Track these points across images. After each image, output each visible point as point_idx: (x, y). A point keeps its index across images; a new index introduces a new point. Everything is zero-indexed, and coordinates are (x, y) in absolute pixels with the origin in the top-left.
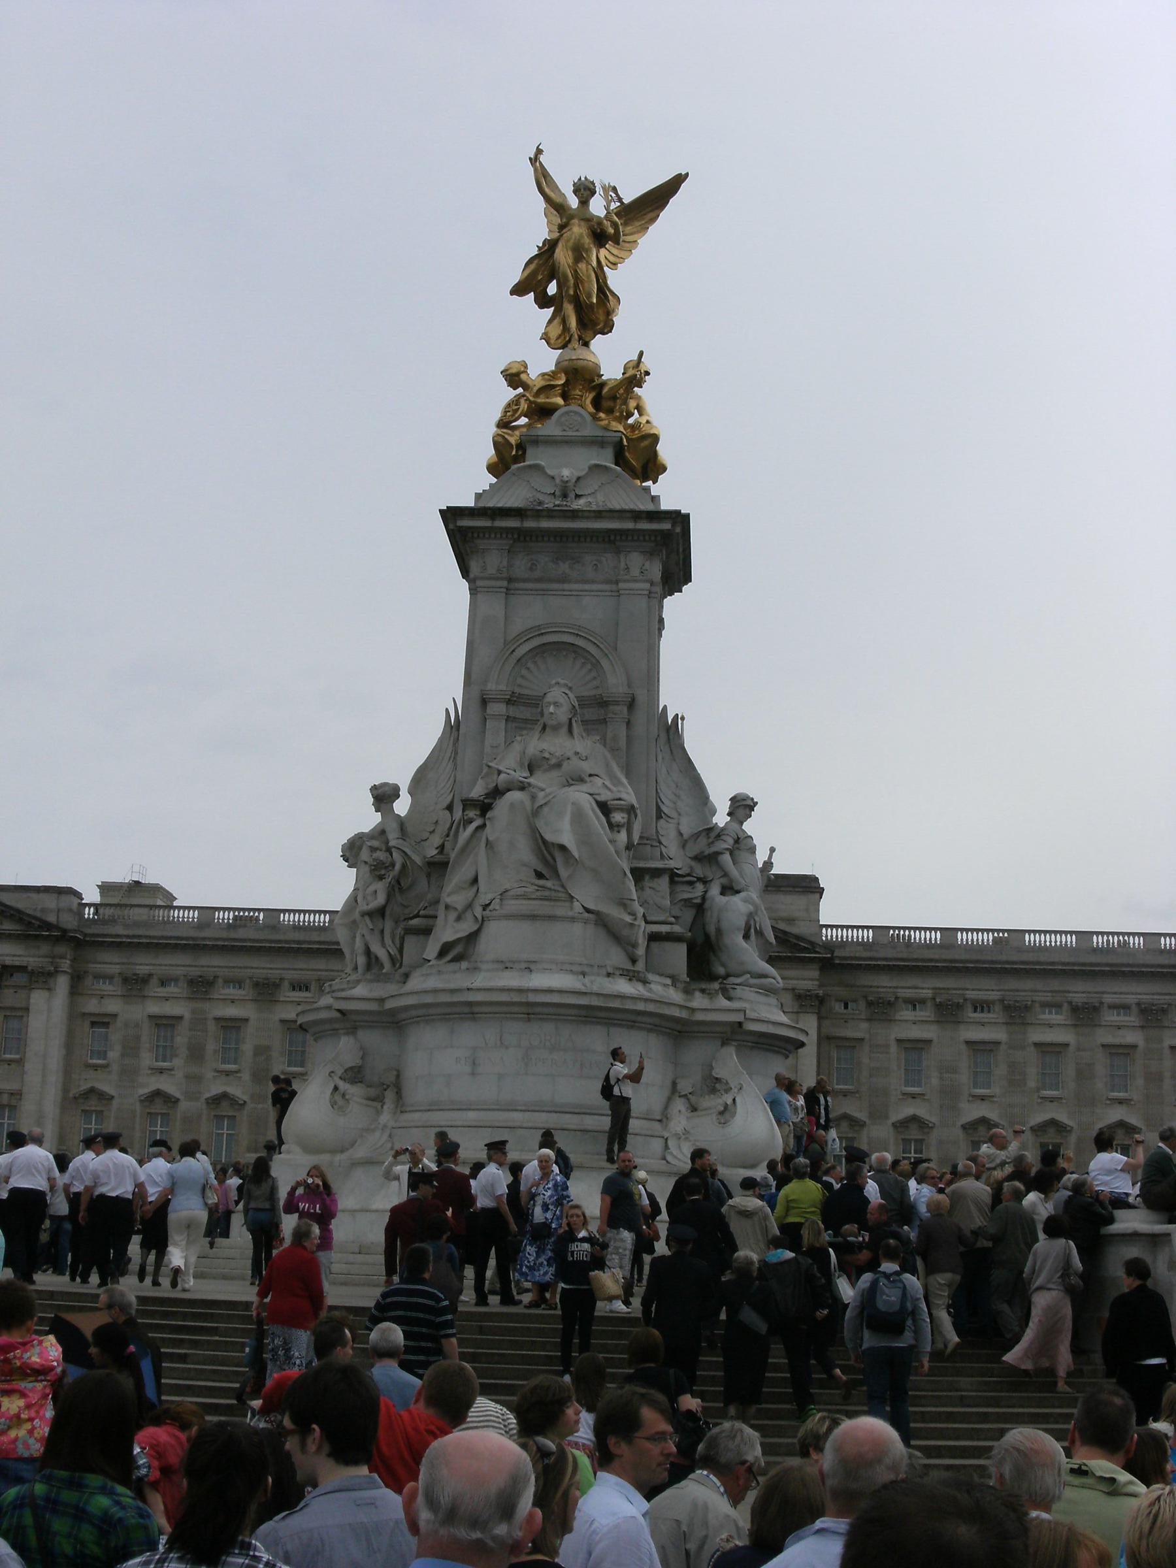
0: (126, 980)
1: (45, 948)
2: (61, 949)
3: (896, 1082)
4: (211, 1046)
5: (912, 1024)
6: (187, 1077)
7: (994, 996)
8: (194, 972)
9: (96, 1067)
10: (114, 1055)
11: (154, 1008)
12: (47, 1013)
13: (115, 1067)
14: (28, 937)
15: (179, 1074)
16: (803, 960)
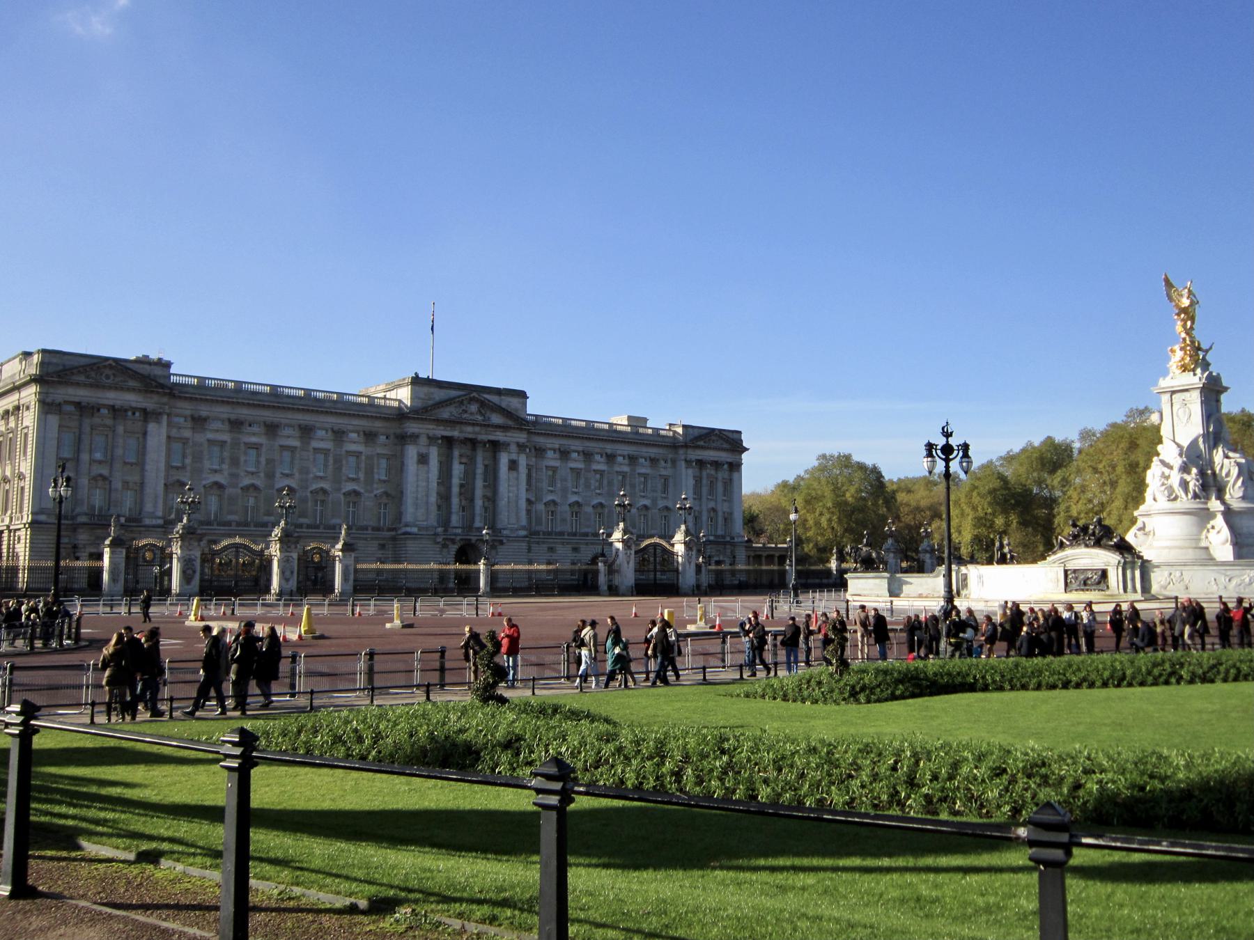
0: (193, 418)
1: (156, 398)
2: (165, 400)
3: (544, 485)
4: (242, 459)
5: (551, 459)
6: (233, 475)
7: (580, 449)
8: (233, 417)
9: (177, 468)
10: (188, 461)
11: (210, 436)
12: (157, 434)
13: (189, 468)
14: (146, 392)
15: (226, 473)
16: (521, 430)
